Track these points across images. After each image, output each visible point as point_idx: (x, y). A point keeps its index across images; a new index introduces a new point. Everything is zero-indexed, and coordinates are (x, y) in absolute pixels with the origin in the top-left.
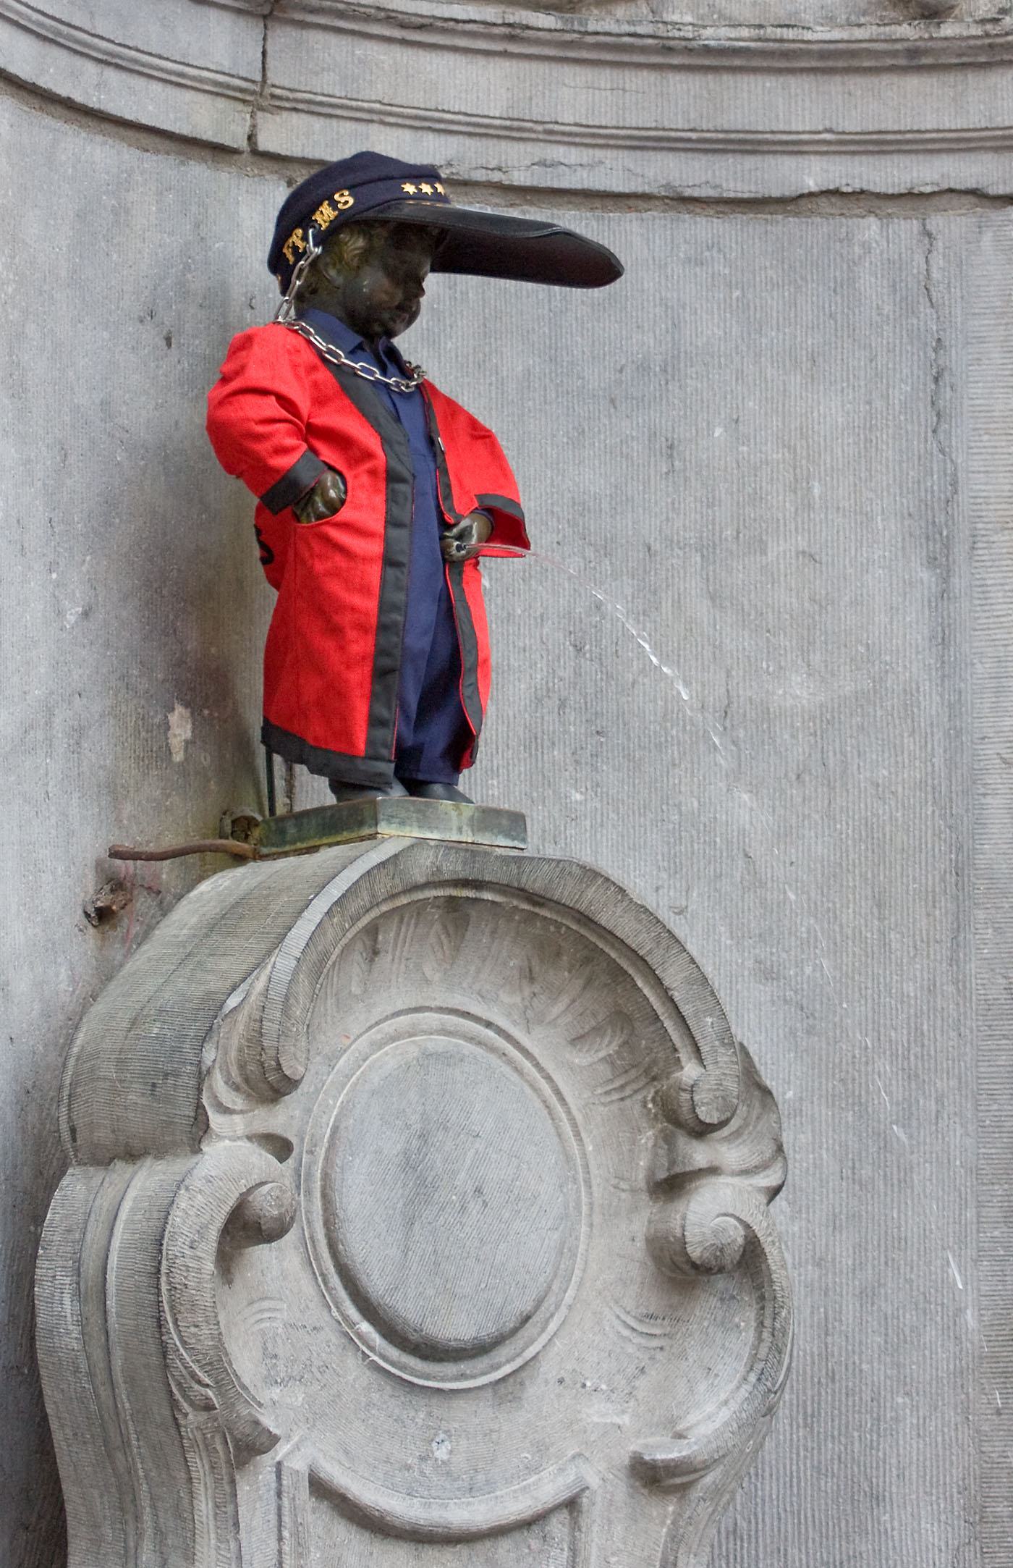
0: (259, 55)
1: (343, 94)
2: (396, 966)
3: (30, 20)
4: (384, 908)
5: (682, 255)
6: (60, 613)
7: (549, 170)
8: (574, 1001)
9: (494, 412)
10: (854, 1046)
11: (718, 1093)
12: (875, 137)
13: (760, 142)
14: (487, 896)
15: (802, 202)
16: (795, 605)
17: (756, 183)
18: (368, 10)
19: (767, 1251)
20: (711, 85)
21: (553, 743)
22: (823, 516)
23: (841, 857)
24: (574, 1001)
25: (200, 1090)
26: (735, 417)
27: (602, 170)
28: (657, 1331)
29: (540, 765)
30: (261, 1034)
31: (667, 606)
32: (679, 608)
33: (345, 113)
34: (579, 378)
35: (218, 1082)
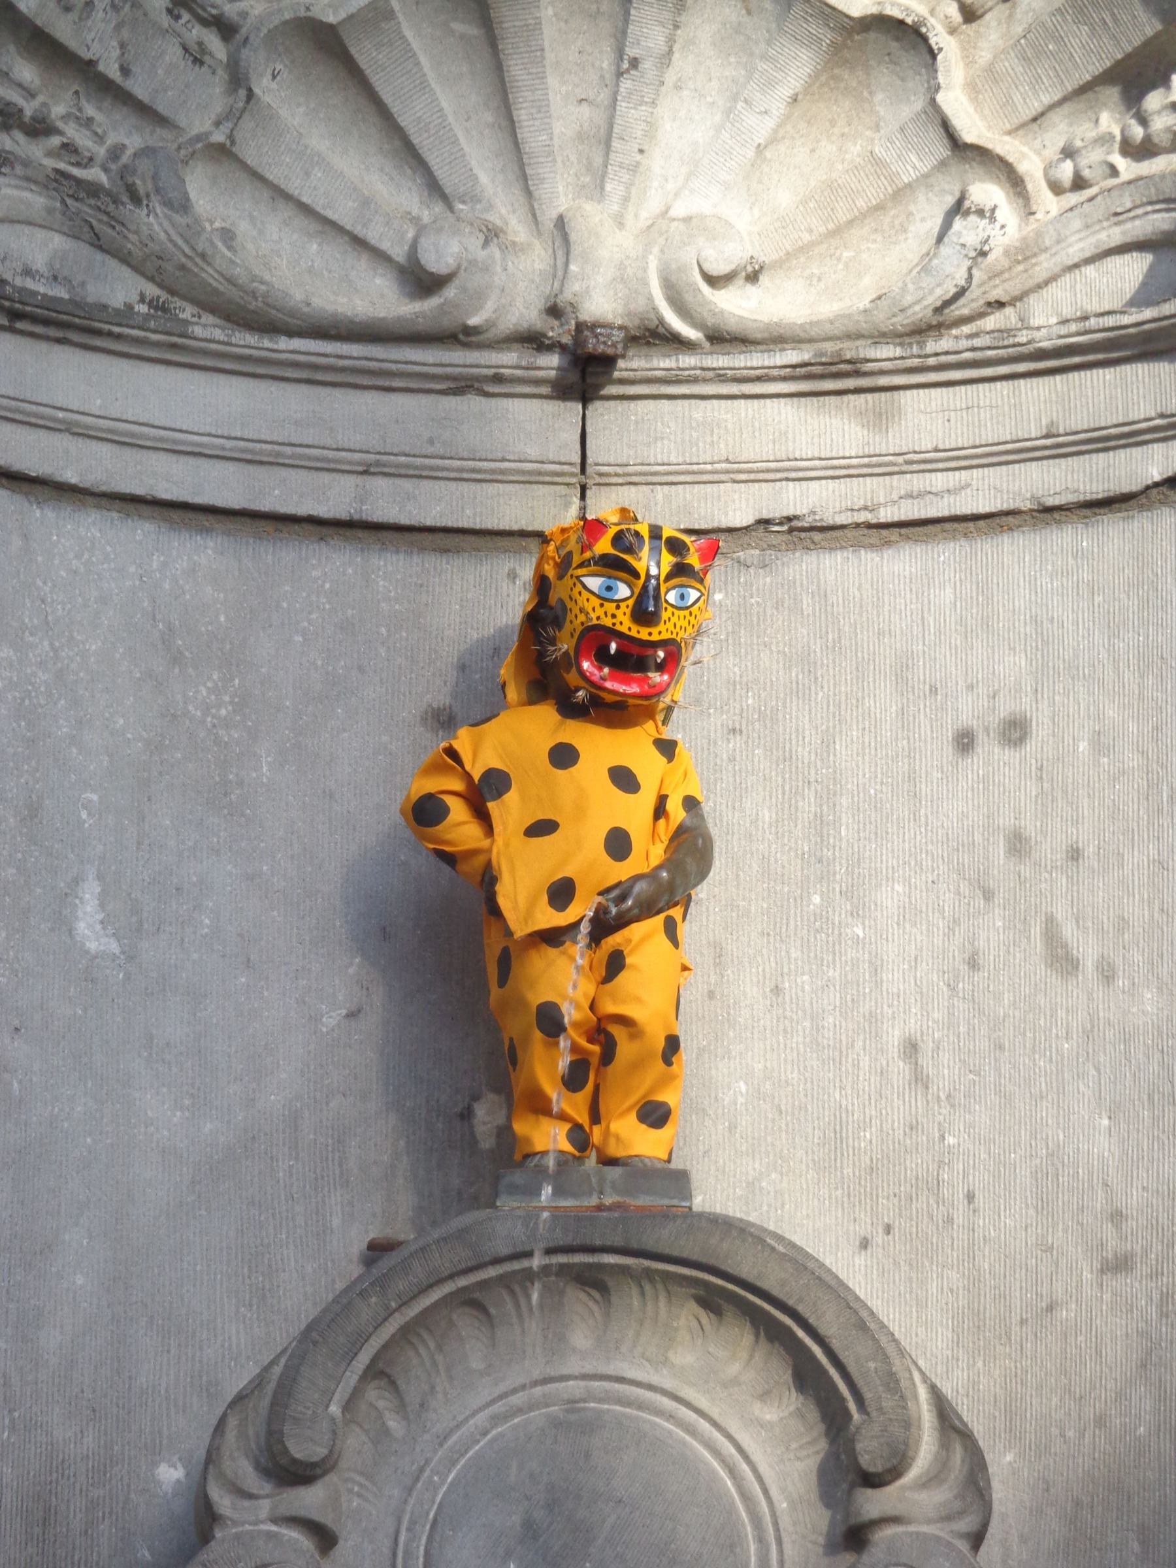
1: (681, 460)
3: (224, 449)
5: (1050, 567)
7: (915, 502)
9: (867, 758)
11: (882, 1440)
18: (692, 372)
21: (927, 1088)
29: (913, 1109)
33: (689, 478)
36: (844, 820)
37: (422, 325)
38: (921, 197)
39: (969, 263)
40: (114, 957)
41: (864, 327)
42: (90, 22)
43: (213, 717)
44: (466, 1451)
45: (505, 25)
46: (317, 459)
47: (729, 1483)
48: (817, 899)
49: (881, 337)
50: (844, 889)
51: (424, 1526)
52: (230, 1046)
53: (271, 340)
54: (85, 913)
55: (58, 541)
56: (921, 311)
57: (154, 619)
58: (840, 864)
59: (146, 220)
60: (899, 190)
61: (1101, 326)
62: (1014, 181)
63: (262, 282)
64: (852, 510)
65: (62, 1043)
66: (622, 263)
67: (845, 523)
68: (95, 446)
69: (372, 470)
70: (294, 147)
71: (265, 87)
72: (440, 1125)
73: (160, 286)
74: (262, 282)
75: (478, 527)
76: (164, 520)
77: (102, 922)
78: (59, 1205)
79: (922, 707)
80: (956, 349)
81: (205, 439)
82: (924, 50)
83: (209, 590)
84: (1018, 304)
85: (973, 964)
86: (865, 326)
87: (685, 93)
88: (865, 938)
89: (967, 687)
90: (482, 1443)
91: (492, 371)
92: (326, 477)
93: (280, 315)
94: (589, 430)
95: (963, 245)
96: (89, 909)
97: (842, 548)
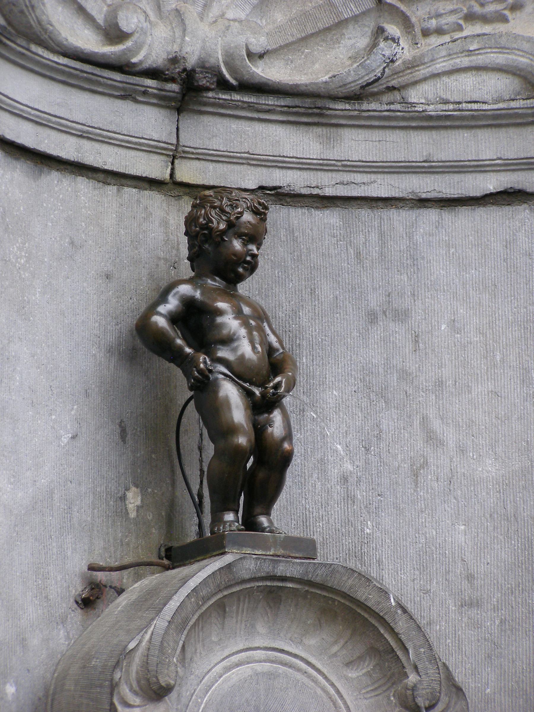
0: (176, 130)
1: (225, 149)
2: (239, 625)
3: (30, 114)
4: (225, 593)
6: (59, 438)
7: (345, 186)
8: (346, 642)
10: (523, 663)
12: (525, 161)
13: (462, 167)
14: (290, 585)
15: (487, 199)
16: (488, 421)
17: (461, 189)
18: (237, 103)
20: (434, 136)
21: (354, 502)
22: (502, 371)
23: (515, 559)
24: (346, 642)
25: (112, 694)
26: (453, 318)
27: (376, 186)
29: (346, 513)
30: (147, 663)
32: (424, 425)
33: (227, 160)
34: (365, 300)
35: (125, 690)
36: (304, 354)
37: (113, 60)
38: (351, 27)
41: (322, 91)
43: (19, 264)
44: (212, 686)
50: (305, 390)
53: (58, 58)
56: (354, 87)
58: (303, 377)
60: (342, 21)
61: (470, 108)
64: (310, 187)
66: (205, 40)
67: (306, 193)
69: (84, 135)
72: (111, 502)
74: (51, 25)
75: (127, 173)
79: (347, 296)
80: (380, 109)
84: (402, 91)
85: (379, 438)
86: (323, 90)
88: (317, 418)
89: (373, 289)
90: (219, 682)
91: (143, 89)
92: (64, 137)
93: (53, 44)
94: (180, 127)
95: (384, 55)
97: (302, 207)
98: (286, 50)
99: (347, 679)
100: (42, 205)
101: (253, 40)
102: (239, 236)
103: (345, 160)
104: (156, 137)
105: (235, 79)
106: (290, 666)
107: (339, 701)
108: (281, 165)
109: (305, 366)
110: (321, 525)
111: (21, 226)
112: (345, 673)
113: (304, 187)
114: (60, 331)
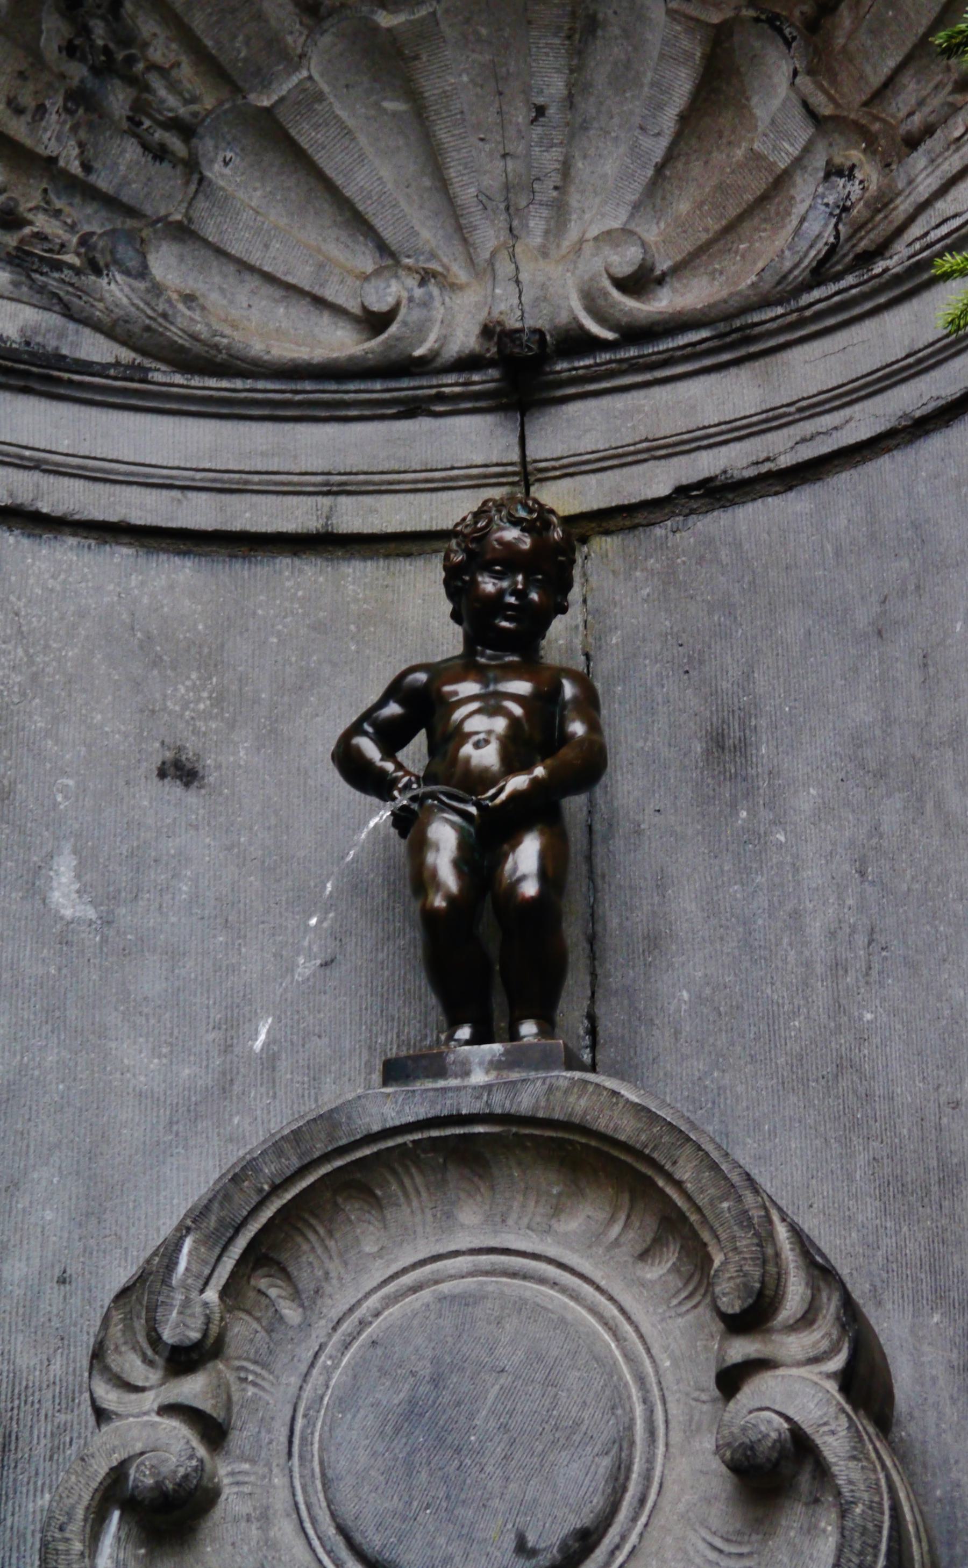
1: (607, 446)
3: (193, 480)
14: (480, 1129)
18: (609, 366)
19: (819, 1441)
21: (846, 971)
24: (628, 1217)
28: (745, 1550)
31: (929, 806)
38: (798, 180)
39: (834, 220)
40: (91, 922)
42: (43, 124)
43: (193, 710)
45: (426, 94)
46: (283, 484)
47: (613, 1345)
48: (744, 814)
49: (766, 303)
51: (318, 1411)
52: (208, 998)
54: (60, 884)
55: (33, 564)
57: (133, 629)
59: (107, 287)
62: (870, 141)
63: (223, 336)
65: (33, 1000)
68: (66, 481)
69: (335, 489)
70: (251, 224)
71: (216, 172)
73: (135, 349)
74: (223, 336)
75: (434, 528)
76: (142, 546)
77: (78, 892)
78: (28, 1146)
81: (174, 472)
82: (780, 42)
83: (187, 602)
86: (755, 299)
87: (592, 132)
90: (374, 1325)
91: (434, 391)
93: (245, 365)
95: (827, 205)
96: (64, 880)
97: (754, 500)
98: (704, 258)
99: (643, 1284)
100: (254, 613)
101: (615, 257)
102: (487, 568)
103: (799, 401)
104: (479, 461)
105: (611, 329)
106: (525, 1276)
107: (628, 1328)
108: (705, 442)
109: (765, 760)
110: (797, 1023)
111: (200, 653)
112: (639, 1273)
113: (748, 467)
114: (296, 801)
